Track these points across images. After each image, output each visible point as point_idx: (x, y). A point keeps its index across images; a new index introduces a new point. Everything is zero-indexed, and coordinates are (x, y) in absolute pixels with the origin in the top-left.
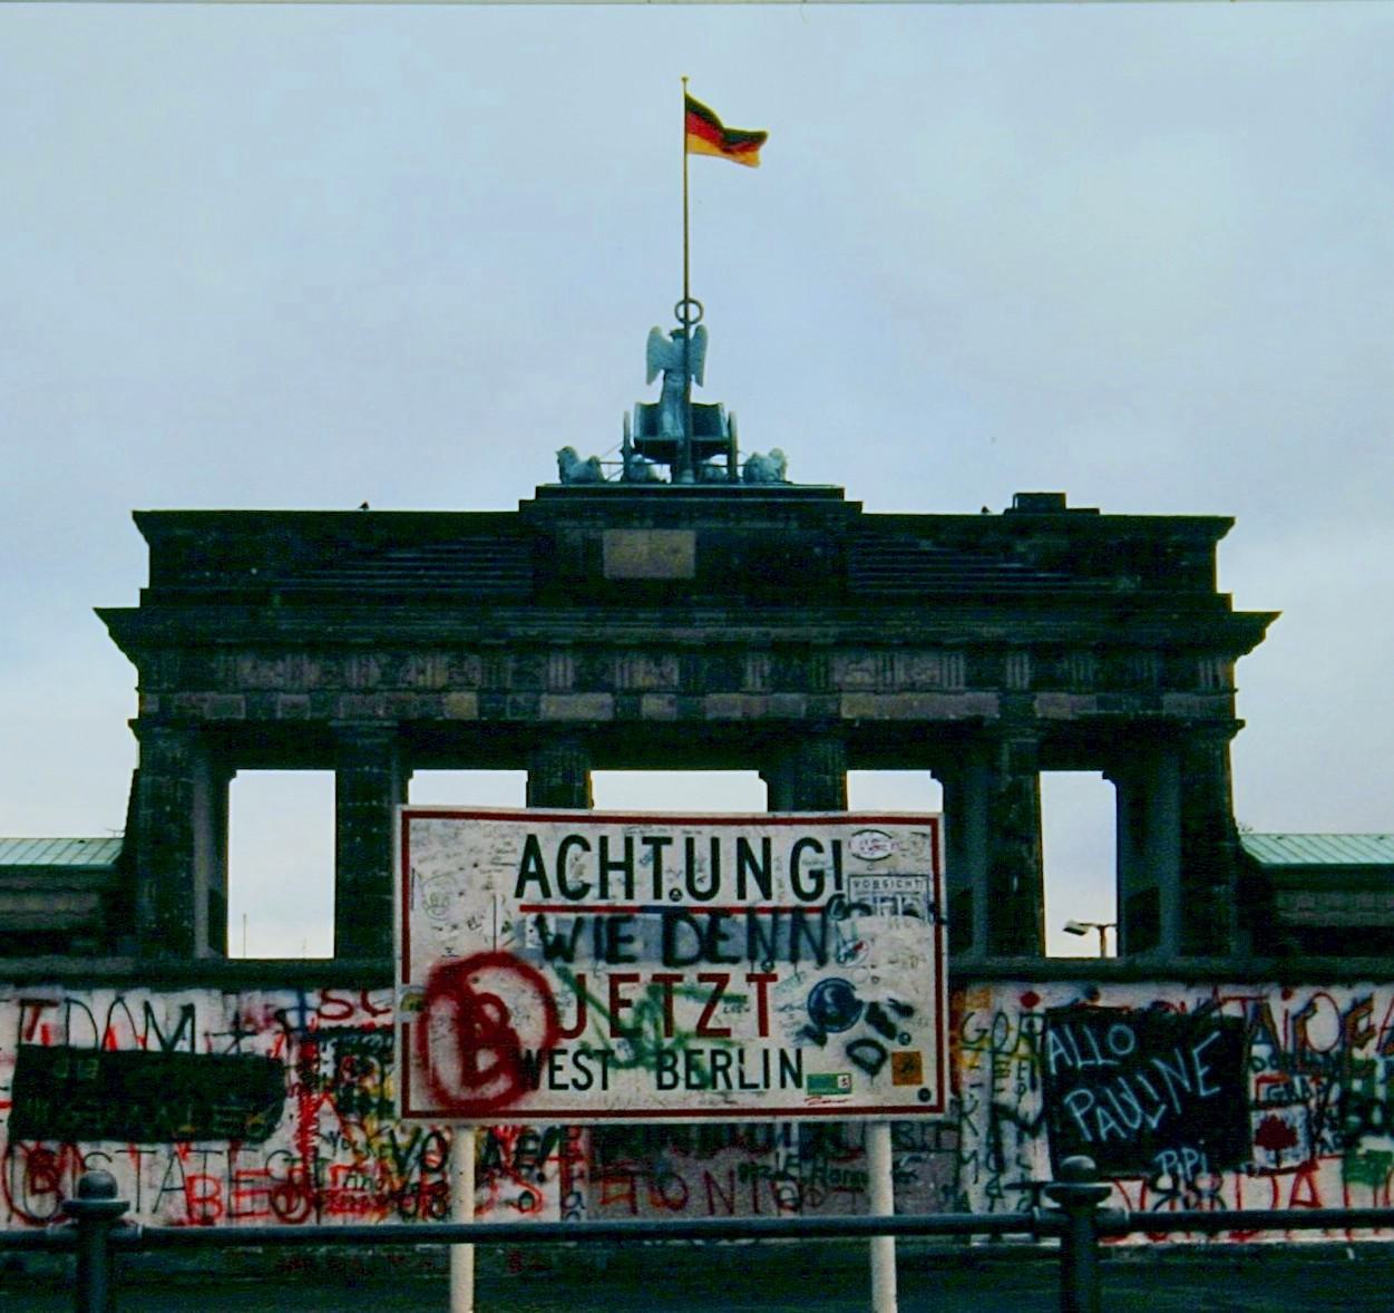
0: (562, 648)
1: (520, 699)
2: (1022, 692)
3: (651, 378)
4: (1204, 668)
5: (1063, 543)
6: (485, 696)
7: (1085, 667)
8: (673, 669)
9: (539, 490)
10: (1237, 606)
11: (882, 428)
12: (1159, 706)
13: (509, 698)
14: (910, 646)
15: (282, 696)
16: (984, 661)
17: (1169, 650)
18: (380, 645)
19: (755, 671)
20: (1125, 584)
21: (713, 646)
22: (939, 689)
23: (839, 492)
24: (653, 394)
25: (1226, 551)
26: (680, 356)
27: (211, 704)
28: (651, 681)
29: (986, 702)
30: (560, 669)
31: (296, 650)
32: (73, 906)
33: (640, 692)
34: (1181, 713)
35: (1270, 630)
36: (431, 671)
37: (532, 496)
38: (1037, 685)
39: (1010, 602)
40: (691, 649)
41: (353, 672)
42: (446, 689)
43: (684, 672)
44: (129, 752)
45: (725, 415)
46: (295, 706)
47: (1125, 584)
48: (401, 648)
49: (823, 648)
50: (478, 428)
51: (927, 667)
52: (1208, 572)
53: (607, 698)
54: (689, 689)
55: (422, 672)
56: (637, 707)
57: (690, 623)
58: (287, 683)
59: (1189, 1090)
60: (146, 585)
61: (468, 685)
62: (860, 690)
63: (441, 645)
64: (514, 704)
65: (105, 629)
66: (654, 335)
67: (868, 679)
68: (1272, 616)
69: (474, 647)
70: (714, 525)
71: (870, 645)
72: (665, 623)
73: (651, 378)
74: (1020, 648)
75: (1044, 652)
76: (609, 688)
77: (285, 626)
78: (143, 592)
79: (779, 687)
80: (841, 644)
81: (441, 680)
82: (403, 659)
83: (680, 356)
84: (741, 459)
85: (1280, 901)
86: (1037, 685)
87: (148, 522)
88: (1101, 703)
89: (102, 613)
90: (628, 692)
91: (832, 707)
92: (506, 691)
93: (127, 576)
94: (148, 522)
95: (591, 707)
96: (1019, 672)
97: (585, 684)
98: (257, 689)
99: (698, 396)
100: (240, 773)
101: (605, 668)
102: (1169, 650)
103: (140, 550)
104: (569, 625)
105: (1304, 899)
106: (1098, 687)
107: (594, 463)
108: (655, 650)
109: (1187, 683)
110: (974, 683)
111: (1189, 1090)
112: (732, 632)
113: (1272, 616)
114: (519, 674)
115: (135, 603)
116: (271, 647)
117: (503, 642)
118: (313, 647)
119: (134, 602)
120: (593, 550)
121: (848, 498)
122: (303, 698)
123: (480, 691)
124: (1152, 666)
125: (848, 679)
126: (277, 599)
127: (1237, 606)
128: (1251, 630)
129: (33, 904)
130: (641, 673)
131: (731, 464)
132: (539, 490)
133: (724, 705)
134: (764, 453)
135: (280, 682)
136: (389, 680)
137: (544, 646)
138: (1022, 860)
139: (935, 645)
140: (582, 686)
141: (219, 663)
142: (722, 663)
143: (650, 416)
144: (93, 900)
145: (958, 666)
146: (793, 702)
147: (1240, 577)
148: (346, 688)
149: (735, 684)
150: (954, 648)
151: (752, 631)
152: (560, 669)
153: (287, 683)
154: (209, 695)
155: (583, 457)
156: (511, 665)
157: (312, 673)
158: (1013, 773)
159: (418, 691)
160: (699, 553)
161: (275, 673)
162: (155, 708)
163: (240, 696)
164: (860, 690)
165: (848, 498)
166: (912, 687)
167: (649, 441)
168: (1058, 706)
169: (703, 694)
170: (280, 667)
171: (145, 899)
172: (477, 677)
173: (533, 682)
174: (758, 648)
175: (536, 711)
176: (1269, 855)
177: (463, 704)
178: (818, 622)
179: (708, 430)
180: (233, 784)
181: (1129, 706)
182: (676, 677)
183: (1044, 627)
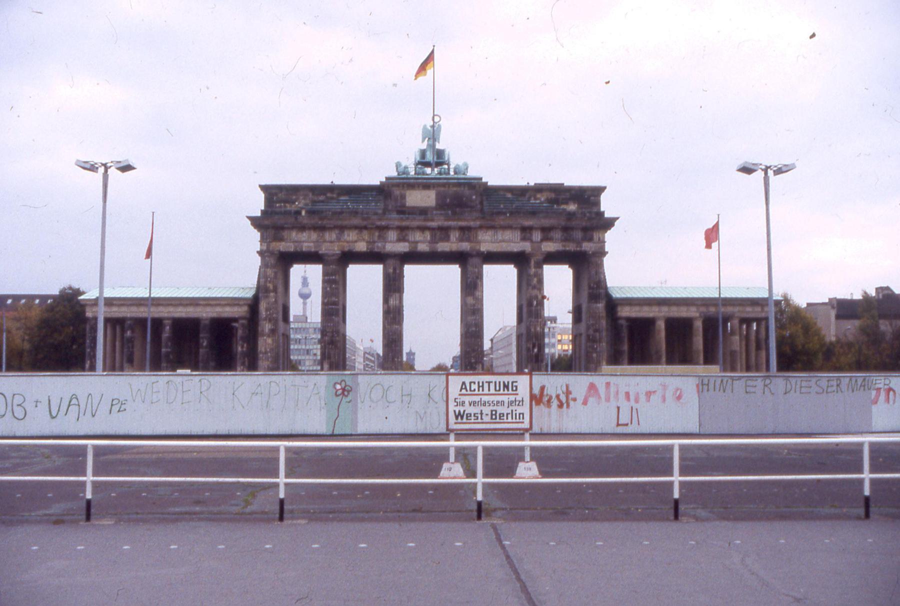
0: (392, 228)
1: (380, 245)
3: (423, 141)
4: (596, 236)
5: (553, 195)
7: (557, 235)
8: (428, 235)
9: (387, 178)
10: (606, 215)
11: (497, 158)
12: (581, 247)
14: (504, 228)
15: (305, 244)
16: (526, 231)
17: (585, 230)
18: (335, 227)
19: (454, 235)
20: (572, 207)
21: (441, 229)
22: (512, 242)
23: (481, 179)
24: (424, 146)
25: (603, 197)
26: (432, 134)
27: (283, 246)
28: (421, 238)
29: (526, 247)
30: (392, 235)
31: (310, 229)
32: (240, 310)
33: (417, 242)
34: (587, 249)
35: (616, 223)
36: (351, 236)
37: (384, 180)
38: (542, 240)
39: (533, 213)
41: (327, 236)
42: (356, 242)
43: (431, 236)
44: (257, 261)
45: (447, 153)
46: (309, 247)
47: (572, 207)
48: (342, 229)
49: (475, 228)
50: (368, 157)
51: (508, 235)
52: (598, 204)
53: (407, 244)
54: (433, 241)
55: (349, 235)
56: (416, 248)
57: (432, 220)
58: (307, 241)
60: (263, 208)
61: (364, 240)
62: (487, 242)
63: (356, 227)
64: (378, 247)
65: (249, 222)
66: (425, 127)
67: (489, 238)
68: (618, 218)
69: (366, 228)
70: (442, 189)
71: (492, 227)
72: (425, 220)
73: (423, 141)
74: (536, 229)
75: (546, 231)
76: (407, 241)
77: (305, 221)
79: (461, 240)
80: (481, 227)
81: (355, 238)
82: (343, 232)
83: (432, 134)
84: (452, 166)
85: (619, 309)
86: (542, 240)
87: (265, 188)
88: (564, 246)
90: (413, 242)
91: (478, 248)
92: (374, 242)
93: (257, 204)
94: (265, 188)
95: (402, 247)
96: (537, 236)
97: (402, 239)
98: (296, 242)
99: (438, 146)
101: (406, 235)
102: (585, 230)
103: (261, 196)
104: (394, 219)
105: (627, 308)
106: (562, 241)
107: (406, 167)
108: (422, 229)
109: (591, 239)
110: (524, 239)
112: (447, 224)
113: (618, 218)
114: (379, 237)
115: (259, 215)
116: (302, 228)
118: (315, 228)
119: (259, 215)
120: (403, 197)
121: (484, 180)
122: (312, 244)
123: (367, 242)
124: (579, 235)
126: (303, 213)
127: (606, 215)
128: (609, 224)
129: (228, 309)
130: (418, 236)
131: (449, 169)
132: (387, 178)
133: (443, 247)
134: (461, 164)
135: (303, 239)
136: (339, 239)
137: (387, 228)
138: (536, 297)
139: (510, 227)
140: (400, 240)
141: (285, 234)
142: (443, 232)
143: (423, 153)
144: (245, 308)
145: (517, 234)
146: (465, 246)
147: (608, 206)
148: (325, 241)
149: (447, 239)
150: (516, 228)
152: (392, 235)
153: (307, 241)
154: (283, 243)
155: (403, 165)
156: (377, 234)
157: (314, 236)
158: (535, 267)
159: (348, 242)
160: (437, 199)
161: (304, 236)
162: (265, 248)
163: (291, 244)
164: (487, 242)
165: (484, 180)
166: (503, 241)
167: (423, 163)
168: (550, 247)
170: (304, 234)
171: (263, 306)
172: (366, 237)
173: (382, 238)
174: (454, 228)
175: (384, 248)
176: (616, 294)
177: (361, 247)
178: (474, 220)
179: (440, 159)
180: (292, 270)
181: (571, 247)
182: (429, 238)
183: (546, 222)
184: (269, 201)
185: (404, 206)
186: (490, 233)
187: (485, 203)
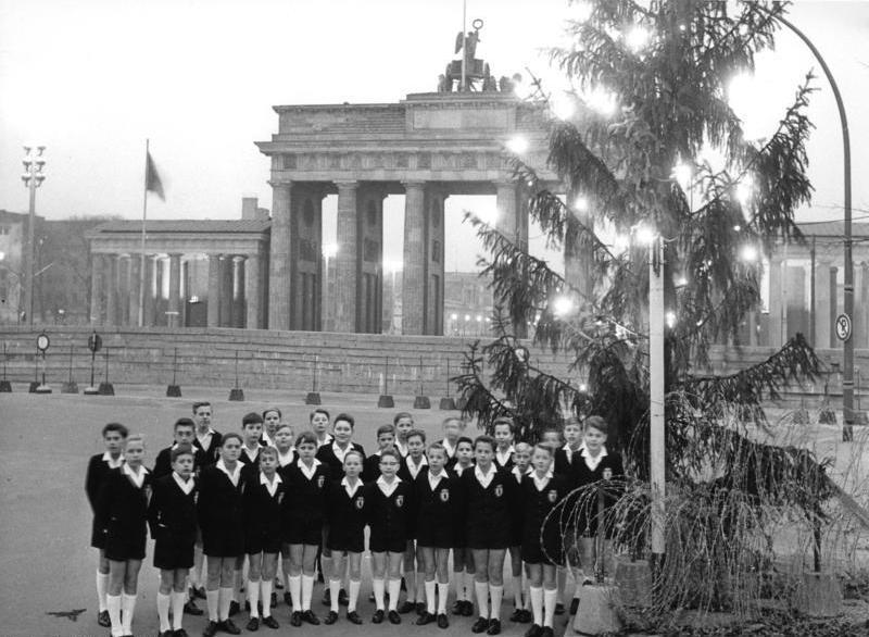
26: (467, 42)
30: (413, 162)
37: (405, 98)
40: (458, 154)
45: (485, 63)
59: (197, 493)
73: (457, 51)
78: (273, 136)
83: (467, 42)
89: (256, 143)
93: (270, 126)
95: (425, 176)
97: (425, 165)
100: (451, 196)
103: (276, 116)
111: (197, 493)
132: (408, 96)
151: (478, 148)
152: (413, 162)
184: (282, 124)
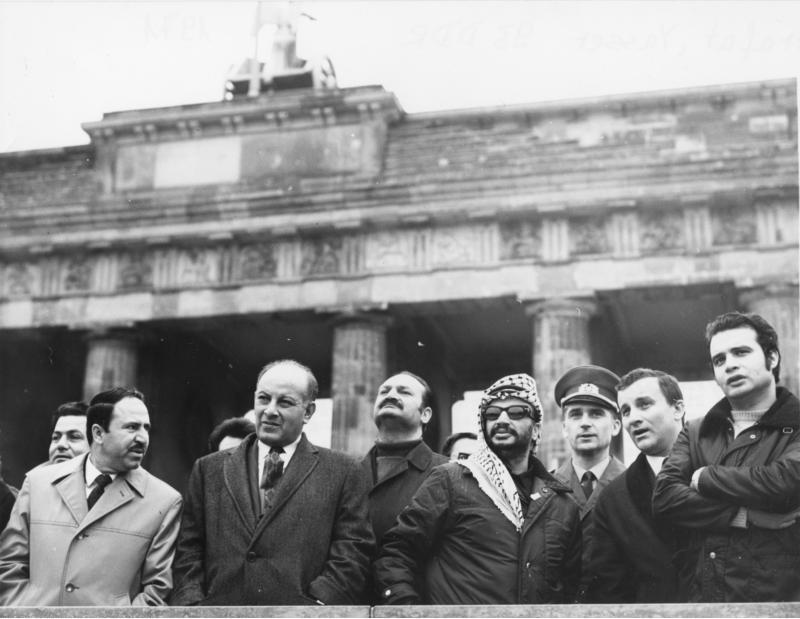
2: (559, 264)
6: (39, 305)
13: (61, 304)
21: (240, 241)
28: (191, 279)
29: (522, 282)
33: (174, 291)
38: (573, 258)
43: (221, 268)
49: (352, 232)
53: (146, 299)
56: (175, 306)
57: (214, 215)
79: (309, 278)
80: (369, 228)
95: (136, 309)
97: (135, 284)
109: (748, 241)
117: (48, 249)
125: (380, 263)
149: (265, 271)
150: (485, 221)
169: (237, 287)
182: (213, 275)
185: (149, 188)
186: (406, 242)
187: (392, 162)
